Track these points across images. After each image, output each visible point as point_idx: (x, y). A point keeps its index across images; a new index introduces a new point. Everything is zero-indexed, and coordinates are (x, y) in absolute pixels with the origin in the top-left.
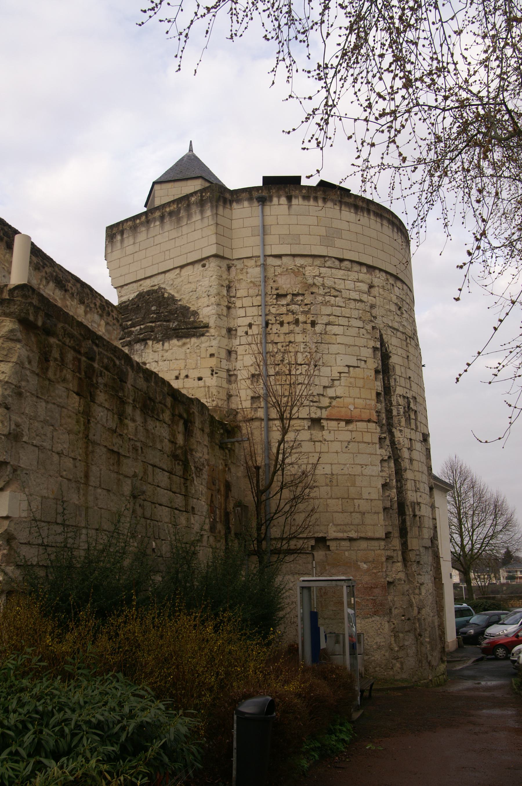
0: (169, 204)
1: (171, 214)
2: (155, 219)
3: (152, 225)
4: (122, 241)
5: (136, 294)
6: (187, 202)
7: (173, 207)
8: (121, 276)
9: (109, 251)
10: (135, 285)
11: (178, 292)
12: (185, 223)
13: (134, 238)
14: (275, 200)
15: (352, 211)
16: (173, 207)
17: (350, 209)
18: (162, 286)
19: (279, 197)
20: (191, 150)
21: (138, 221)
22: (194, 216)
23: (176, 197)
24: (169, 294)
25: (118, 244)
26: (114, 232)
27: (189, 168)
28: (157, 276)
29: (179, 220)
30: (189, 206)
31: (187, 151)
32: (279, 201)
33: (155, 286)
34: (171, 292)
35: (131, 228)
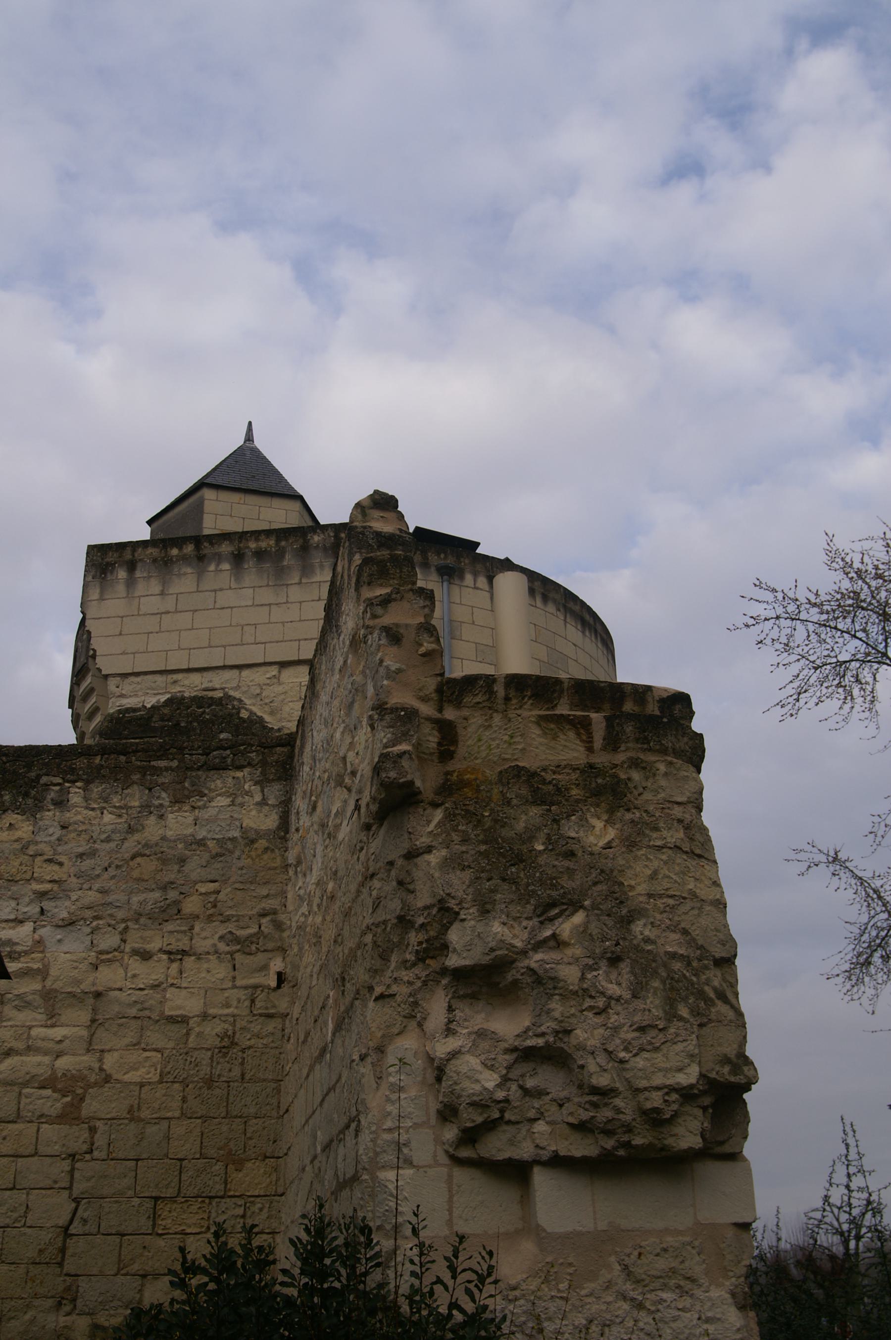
0: (256, 534)
1: (260, 555)
2: (219, 558)
3: (212, 567)
4: (131, 583)
5: (163, 699)
6: (301, 541)
7: (268, 543)
8: (124, 653)
9: (95, 594)
10: (159, 679)
11: (272, 713)
12: (296, 580)
13: (164, 583)
14: (469, 578)
15: (579, 627)
16: (268, 543)
17: (576, 623)
18: (231, 693)
19: (475, 575)
20: (249, 437)
21: (175, 552)
22: (318, 571)
23: (275, 526)
24: (252, 713)
25: (121, 588)
26: (106, 562)
27: (247, 472)
28: (221, 672)
29: (280, 572)
30: (305, 549)
31: (240, 441)
32: (475, 581)
33: (214, 690)
34: (254, 709)
35: (155, 561)
